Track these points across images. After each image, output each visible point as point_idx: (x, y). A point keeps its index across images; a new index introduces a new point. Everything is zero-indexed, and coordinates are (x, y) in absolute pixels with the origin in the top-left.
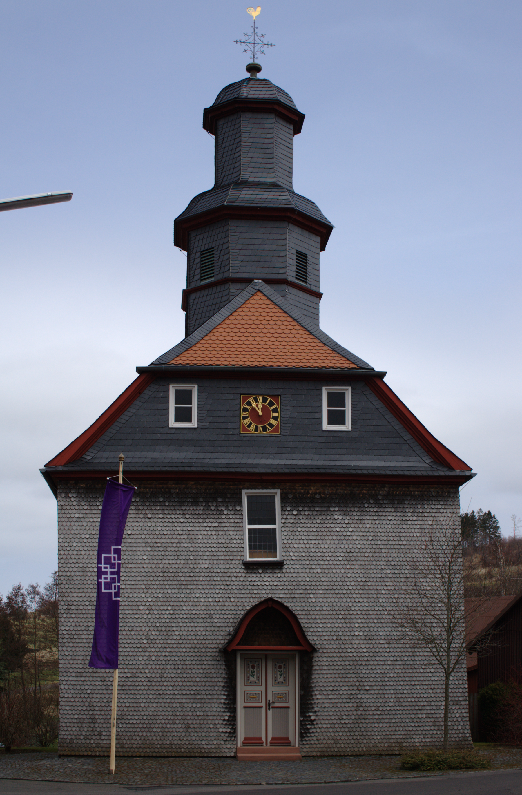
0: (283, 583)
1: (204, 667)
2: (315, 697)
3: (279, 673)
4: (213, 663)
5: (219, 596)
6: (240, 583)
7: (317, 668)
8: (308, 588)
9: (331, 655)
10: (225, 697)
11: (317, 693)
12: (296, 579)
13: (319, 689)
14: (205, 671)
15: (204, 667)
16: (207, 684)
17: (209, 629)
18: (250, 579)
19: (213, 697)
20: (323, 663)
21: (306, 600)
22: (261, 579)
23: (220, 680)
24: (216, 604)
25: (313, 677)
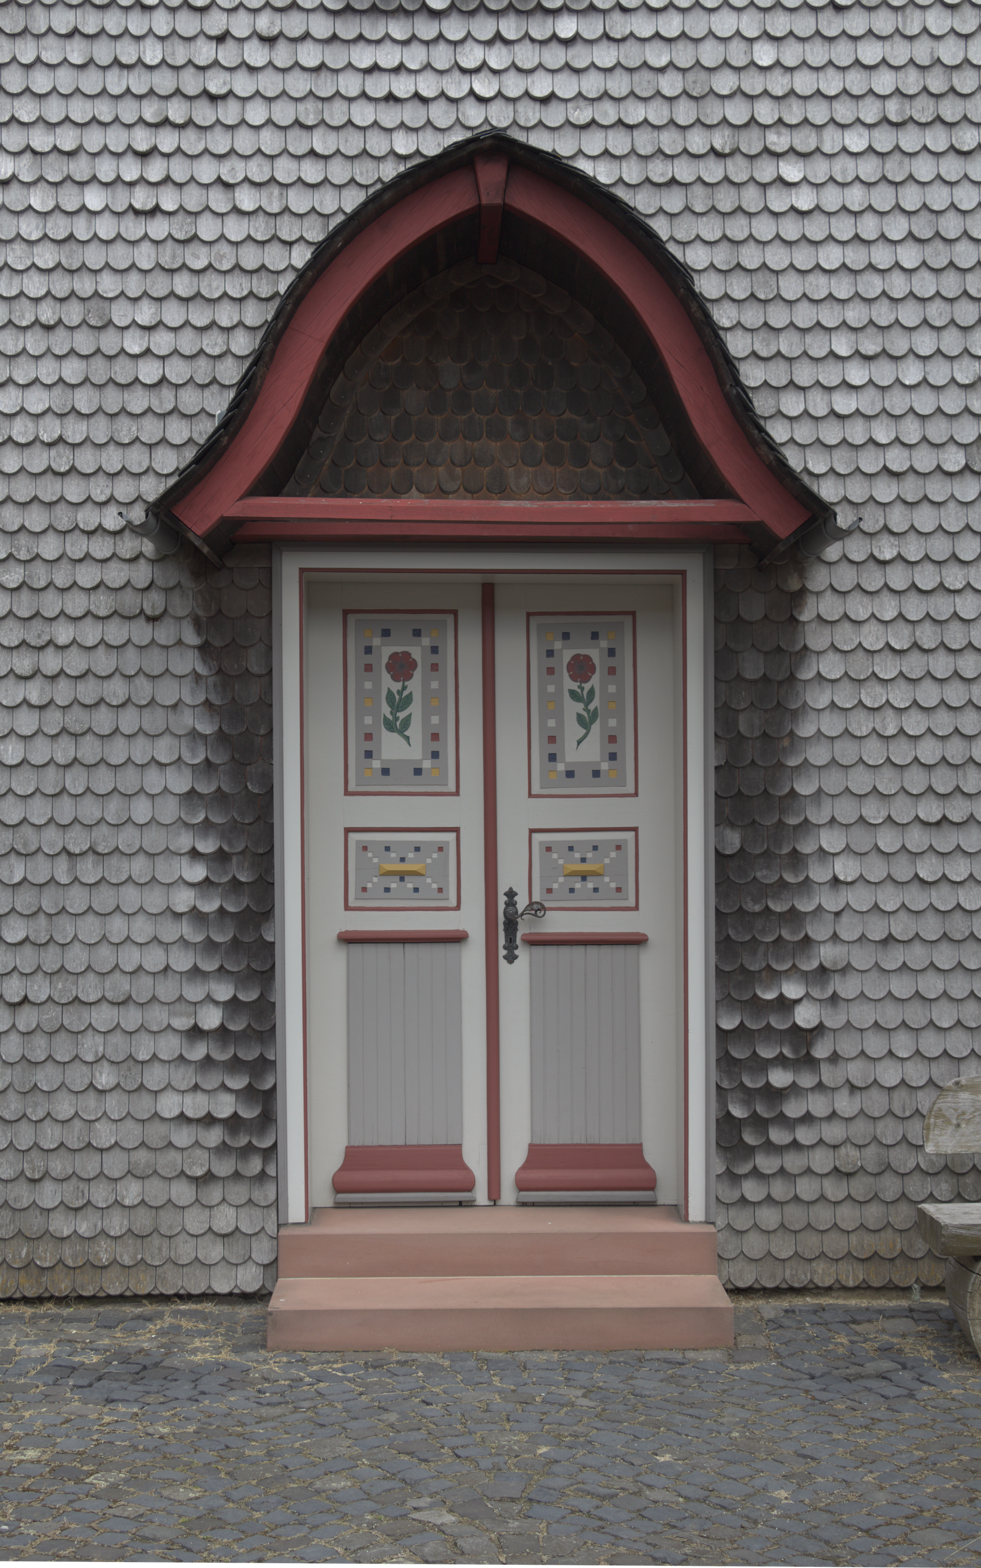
0: (592, 85)
1: (51, 662)
2: (819, 874)
3: (573, 708)
4: (116, 633)
5: (155, 171)
6: (298, 84)
7: (831, 667)
8: (765, 112)
9: (927, 578)
10: (198, 873)
11: (831, 841)
12: (684, 55)
13: (846, 811)
14: (63, 692)
15: (51, 662)
16: (75, 781)
17: (84, 401)
18: (363, 57)
19: (118, 870)
20: (872, 638)
21: (751, 199)
22: (442, 57)
23: (164, 750)
24: (133, 228)
25: (806, 729)
